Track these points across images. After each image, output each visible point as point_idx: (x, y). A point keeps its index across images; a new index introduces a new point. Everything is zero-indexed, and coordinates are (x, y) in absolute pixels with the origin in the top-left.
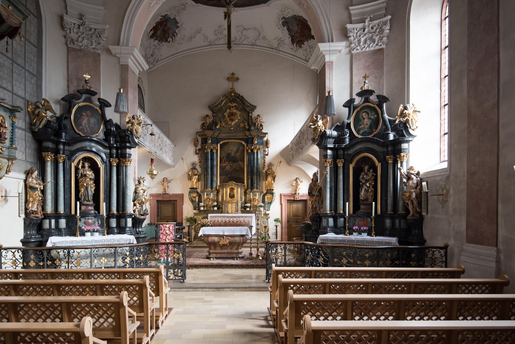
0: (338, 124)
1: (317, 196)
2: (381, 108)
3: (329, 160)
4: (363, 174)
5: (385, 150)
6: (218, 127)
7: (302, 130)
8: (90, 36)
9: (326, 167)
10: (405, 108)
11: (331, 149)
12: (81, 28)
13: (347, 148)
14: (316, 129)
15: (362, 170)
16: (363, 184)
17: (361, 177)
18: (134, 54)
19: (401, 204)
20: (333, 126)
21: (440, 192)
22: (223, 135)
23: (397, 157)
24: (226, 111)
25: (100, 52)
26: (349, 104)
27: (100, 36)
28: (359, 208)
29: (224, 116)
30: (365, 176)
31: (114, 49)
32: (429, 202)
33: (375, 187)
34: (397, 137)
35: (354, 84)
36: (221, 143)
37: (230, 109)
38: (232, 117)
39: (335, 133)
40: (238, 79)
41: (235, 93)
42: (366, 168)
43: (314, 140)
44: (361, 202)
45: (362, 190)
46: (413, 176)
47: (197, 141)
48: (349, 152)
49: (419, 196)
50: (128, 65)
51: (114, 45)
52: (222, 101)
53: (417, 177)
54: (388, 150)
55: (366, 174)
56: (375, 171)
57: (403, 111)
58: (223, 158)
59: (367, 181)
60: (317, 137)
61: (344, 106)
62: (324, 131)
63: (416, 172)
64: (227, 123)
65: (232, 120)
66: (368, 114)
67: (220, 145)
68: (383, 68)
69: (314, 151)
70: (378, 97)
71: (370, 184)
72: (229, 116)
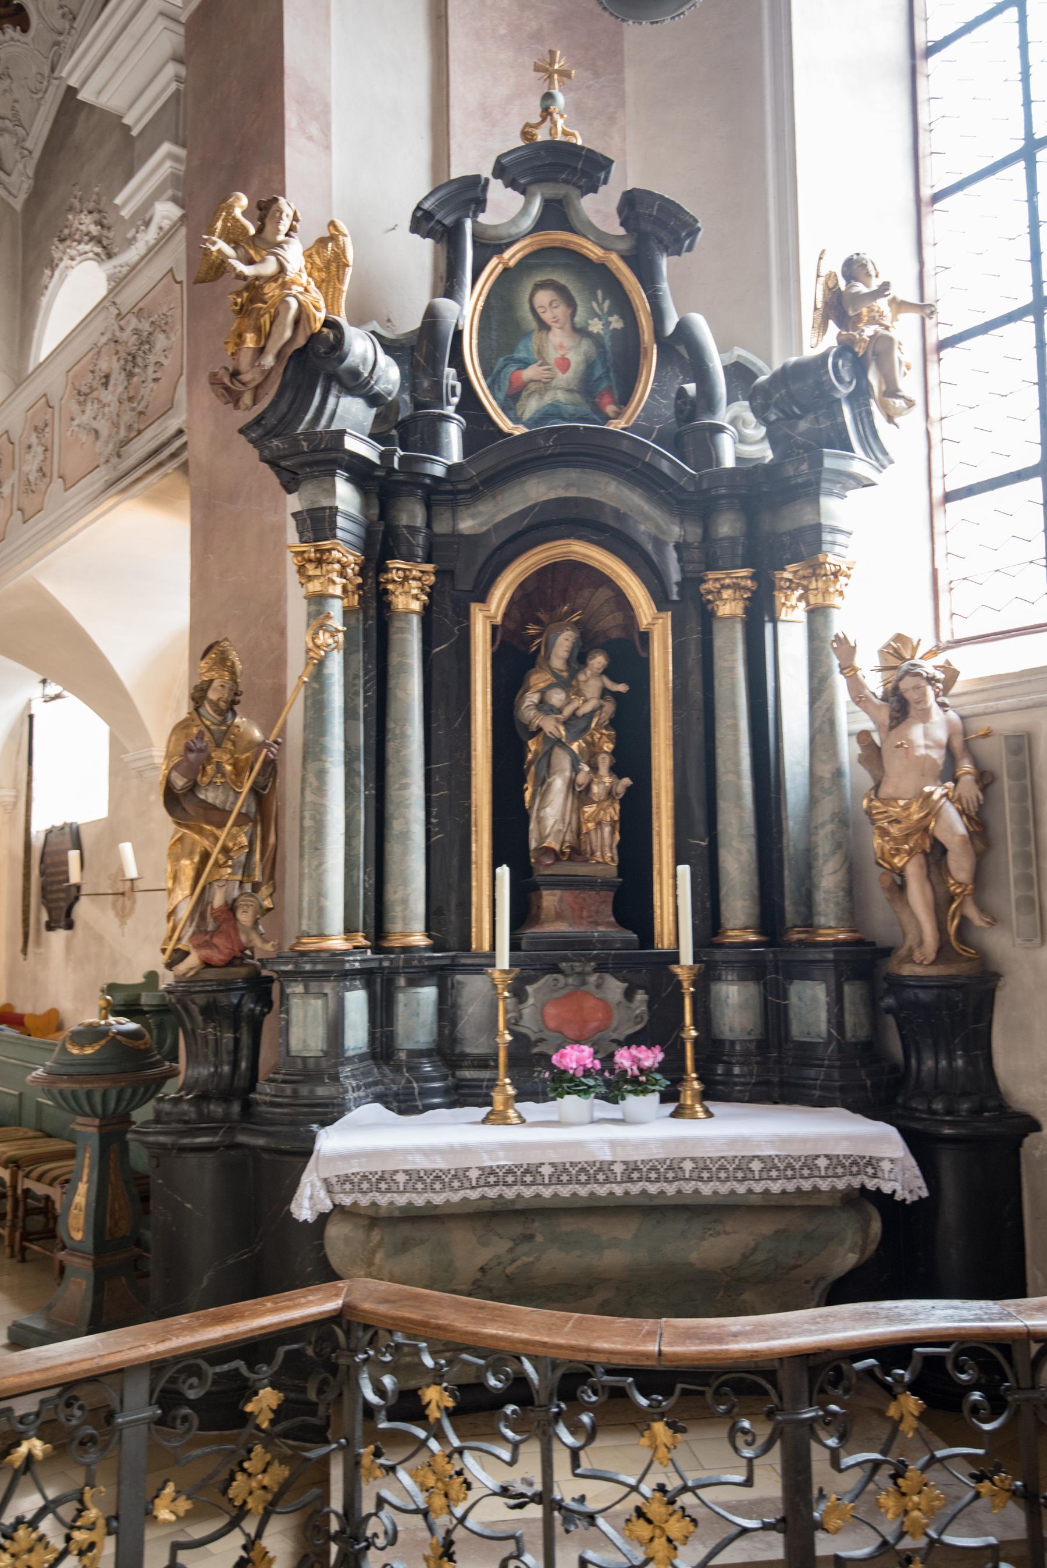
1: (243, 819)
3: (345, 551)
30: (557, 697)
35: (456, 116)
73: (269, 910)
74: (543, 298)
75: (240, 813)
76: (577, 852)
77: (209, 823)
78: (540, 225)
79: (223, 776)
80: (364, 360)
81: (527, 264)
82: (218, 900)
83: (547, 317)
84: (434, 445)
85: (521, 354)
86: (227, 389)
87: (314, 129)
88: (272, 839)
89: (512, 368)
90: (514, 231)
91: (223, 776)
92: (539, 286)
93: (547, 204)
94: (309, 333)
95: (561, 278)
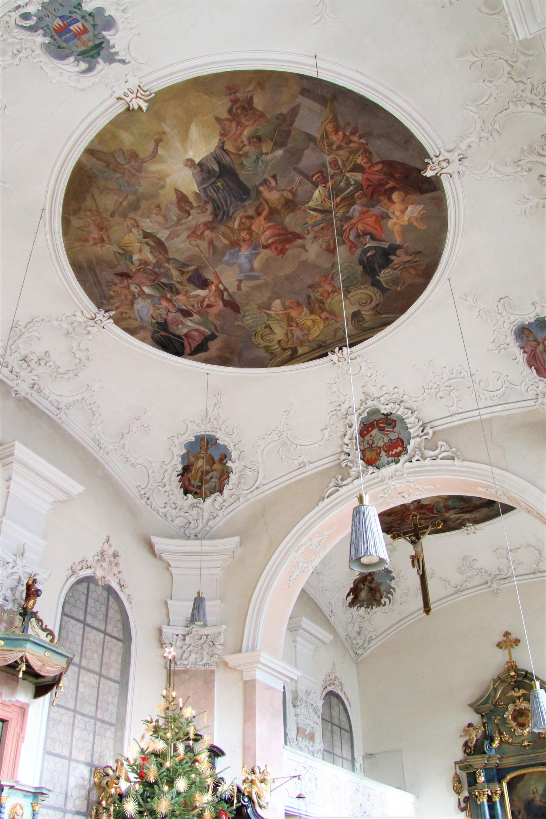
6: (496, 744)
8: (200, 647)
12: (187, 638)
18: (262, 660)
22: (509, 762)
24: (507, 710)
25: (213, 668)
27: (214, 644)
29: (504, 720)
31: (233, 659)
36: (509, 777)
37: (514, 702)
38: (521, 720)
40: (517, 641)
41: (516, 670)
47: (459, 782)
50: (254, 680)
51: (235, 652)
52: (495, 690)
58: (519, 812)
64: (512, 734)
65: (522, 726)
67: (509, 784)
72: (515, 719)
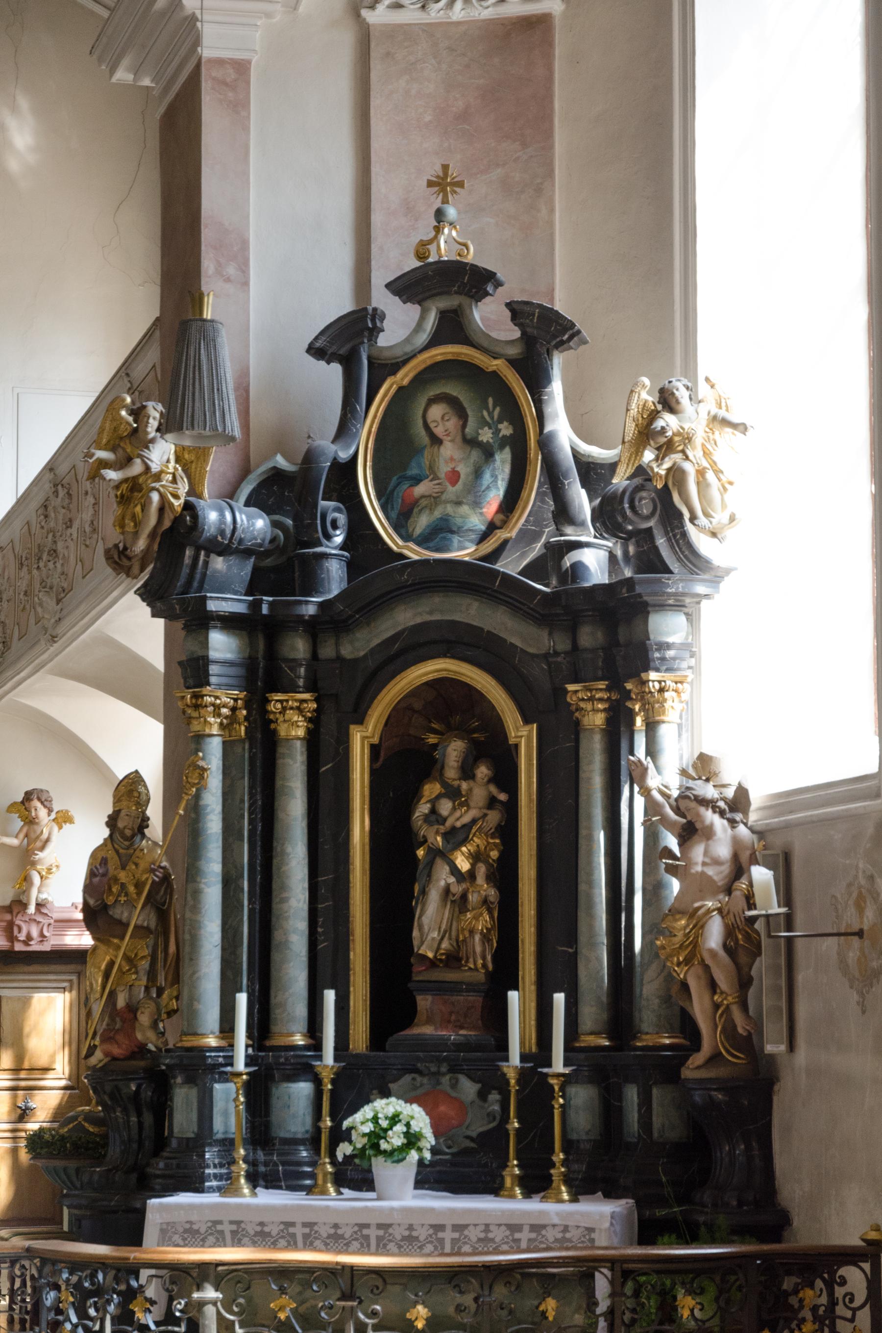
0: (281, 461)
2: (537, 382)
3: (222, 694)
4: (431, 789)
5: (562, 644)
7: (63, 469)
9: (199, 739)
10: (667, 401)
11: (229, 622)
13: (333, 621)
14: (133, 491)
15: (426, 765)
16: (435, 854)
17: (423, 808)
19: (648, 988)
20: (245, 472)
21: (850, 919)
23: (627, 695)
26: (346, 341)
28: (409, 1016)
30: (445, 807)
32: (800, 978)
33: (505, 874)
34: (628, 573)
39: (257, 524)
42: (454, 751)
43: (120, 560)
44: (420, 974)
45: (424, 892)
46: (710, 817)
48: (347, 651)
49: (743, 939)
53: (733, 823)
54: (575, 647)
55: (453, 793)
56: (506, 776)
57: (654, 415)
59: (457, 837)
60: (141, 544)
61: (316, 351)
62: (188, 507)
63: (730, 793)
66: (462, 415)
68: (549, 134)
69: (137, 629)
70: (518, 311)
71: (476, 858)
73: (175, 1011)
74: (436, 412)
75: (136, 927)
76: (453, 959)
77: (114, 937)
78: (433, 342)
79: (126, 895)
80: (222, 532)
81: (423, 379)
82: (121, 1002)
83: (439, 431)
84: (310, 583)
85: (413, 471)
86: (116, 563)
87: (231, 270)
88: (172, 948)
89: (405, 486)
90: (408, 349)
91: (126, 895)
92: (431, 401)
93: (443, 315)
94: (172, 517)
95: (453, 389)
